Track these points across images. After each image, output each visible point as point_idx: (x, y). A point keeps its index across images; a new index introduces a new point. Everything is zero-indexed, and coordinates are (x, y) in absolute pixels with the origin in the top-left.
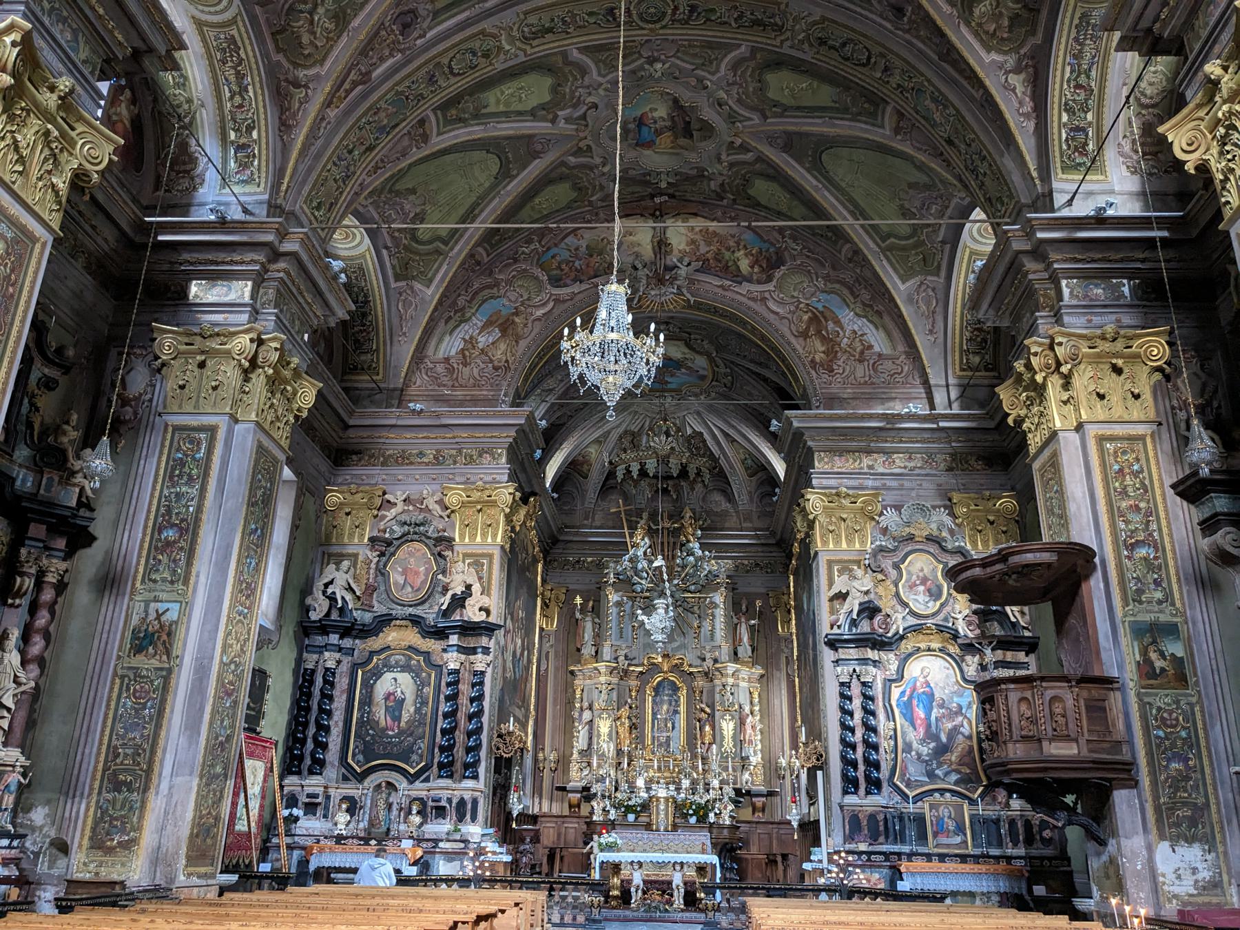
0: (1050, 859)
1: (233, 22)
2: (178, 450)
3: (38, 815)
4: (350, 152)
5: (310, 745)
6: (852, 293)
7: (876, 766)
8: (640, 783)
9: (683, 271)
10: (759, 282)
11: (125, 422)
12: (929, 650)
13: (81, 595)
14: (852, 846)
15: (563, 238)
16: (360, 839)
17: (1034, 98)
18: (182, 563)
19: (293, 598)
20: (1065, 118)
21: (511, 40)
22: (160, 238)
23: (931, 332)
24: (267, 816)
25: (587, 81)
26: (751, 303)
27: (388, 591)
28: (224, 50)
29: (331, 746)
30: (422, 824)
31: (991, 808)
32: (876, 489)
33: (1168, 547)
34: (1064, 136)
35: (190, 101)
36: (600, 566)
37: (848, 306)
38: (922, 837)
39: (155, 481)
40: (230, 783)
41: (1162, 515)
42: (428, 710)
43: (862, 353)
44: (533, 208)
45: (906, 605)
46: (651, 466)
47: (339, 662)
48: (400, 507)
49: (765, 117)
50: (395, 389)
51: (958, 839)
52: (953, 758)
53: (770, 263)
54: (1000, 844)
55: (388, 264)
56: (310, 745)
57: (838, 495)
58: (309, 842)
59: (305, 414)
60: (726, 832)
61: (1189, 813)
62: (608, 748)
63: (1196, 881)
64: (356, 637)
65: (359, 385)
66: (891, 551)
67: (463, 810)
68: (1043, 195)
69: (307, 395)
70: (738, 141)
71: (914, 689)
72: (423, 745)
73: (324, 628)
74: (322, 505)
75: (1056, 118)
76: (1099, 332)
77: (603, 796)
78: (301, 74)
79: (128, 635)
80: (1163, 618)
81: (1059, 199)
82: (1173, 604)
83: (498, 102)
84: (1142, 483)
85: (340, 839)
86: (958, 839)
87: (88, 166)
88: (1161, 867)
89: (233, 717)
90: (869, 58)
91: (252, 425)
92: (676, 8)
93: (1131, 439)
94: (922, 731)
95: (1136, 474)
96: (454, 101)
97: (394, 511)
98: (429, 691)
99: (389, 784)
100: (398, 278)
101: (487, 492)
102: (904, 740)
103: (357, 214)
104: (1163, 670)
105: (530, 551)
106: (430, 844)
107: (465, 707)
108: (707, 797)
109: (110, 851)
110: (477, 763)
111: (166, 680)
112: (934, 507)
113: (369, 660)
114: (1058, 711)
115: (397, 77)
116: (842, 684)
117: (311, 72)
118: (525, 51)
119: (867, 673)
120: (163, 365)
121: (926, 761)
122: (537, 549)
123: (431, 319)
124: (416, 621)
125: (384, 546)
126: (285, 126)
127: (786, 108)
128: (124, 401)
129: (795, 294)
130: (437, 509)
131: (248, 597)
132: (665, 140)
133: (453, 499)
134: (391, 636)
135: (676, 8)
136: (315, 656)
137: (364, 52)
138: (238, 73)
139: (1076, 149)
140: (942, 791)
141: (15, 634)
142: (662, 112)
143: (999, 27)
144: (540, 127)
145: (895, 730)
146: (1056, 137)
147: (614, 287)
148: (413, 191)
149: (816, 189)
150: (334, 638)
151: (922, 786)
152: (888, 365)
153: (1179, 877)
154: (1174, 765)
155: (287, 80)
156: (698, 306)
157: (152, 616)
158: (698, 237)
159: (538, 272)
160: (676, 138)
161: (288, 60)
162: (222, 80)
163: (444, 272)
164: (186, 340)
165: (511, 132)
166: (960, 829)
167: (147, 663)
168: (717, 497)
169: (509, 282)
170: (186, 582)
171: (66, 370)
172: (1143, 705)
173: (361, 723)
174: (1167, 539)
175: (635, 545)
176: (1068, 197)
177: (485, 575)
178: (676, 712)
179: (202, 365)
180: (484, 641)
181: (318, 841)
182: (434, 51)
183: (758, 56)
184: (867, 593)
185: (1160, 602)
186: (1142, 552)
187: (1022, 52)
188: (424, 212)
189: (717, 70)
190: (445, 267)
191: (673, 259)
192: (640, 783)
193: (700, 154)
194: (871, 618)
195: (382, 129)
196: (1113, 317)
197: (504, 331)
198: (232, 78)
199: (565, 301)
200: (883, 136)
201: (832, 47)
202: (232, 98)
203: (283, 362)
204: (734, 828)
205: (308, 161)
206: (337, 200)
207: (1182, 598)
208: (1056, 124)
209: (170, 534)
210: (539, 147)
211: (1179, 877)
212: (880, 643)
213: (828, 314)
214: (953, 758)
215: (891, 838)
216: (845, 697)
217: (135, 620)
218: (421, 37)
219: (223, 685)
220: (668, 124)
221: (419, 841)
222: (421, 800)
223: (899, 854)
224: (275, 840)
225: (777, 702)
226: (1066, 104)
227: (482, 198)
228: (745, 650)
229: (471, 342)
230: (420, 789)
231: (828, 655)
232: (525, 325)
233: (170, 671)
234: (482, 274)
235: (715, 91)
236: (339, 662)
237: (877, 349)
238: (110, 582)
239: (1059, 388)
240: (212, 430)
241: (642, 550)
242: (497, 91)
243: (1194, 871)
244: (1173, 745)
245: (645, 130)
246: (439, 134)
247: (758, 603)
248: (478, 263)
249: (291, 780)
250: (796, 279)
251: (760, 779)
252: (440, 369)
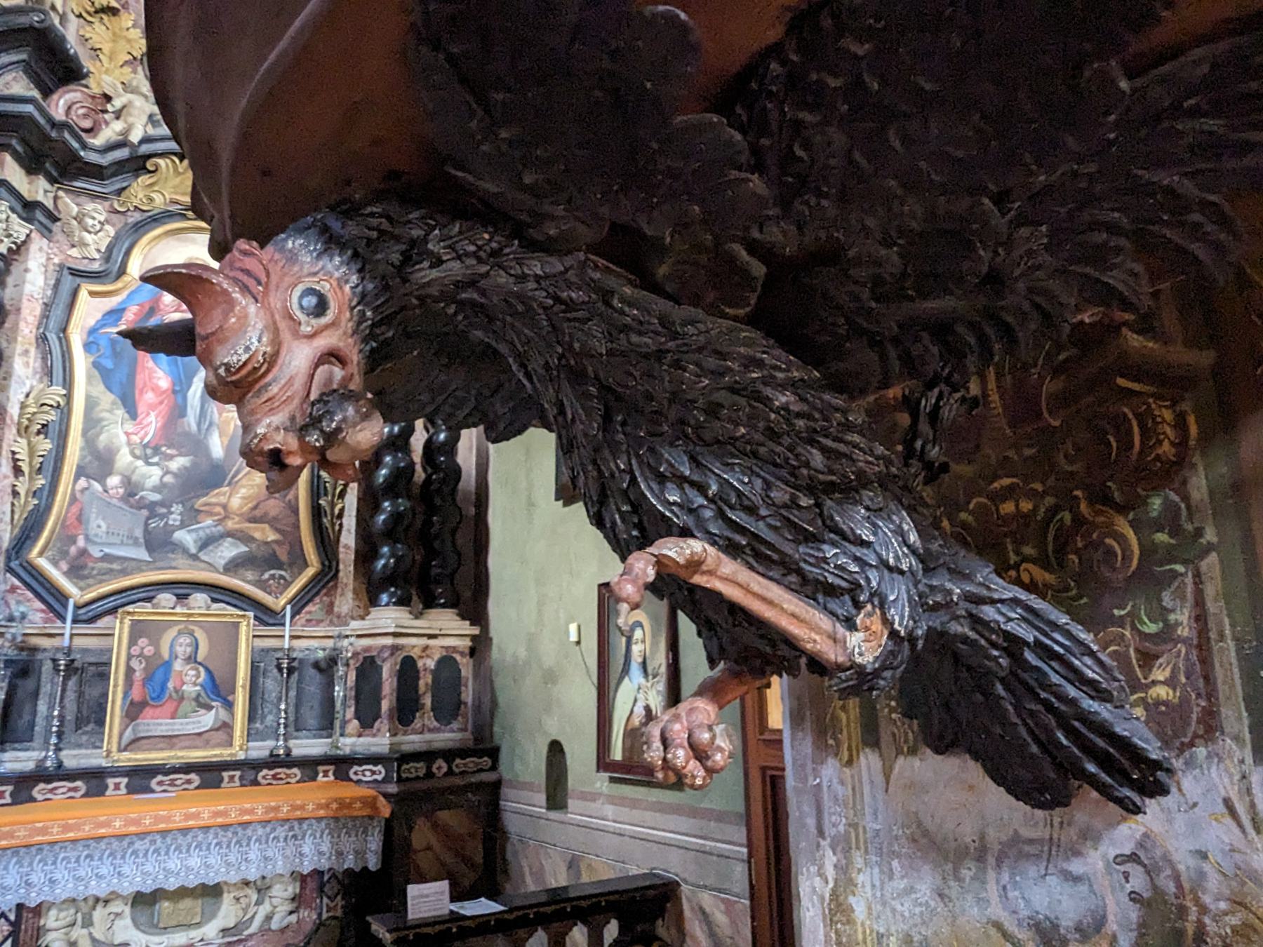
0: (449, 755)
31: (320, 630)
51: (207, 720)
52: (235, 502)
86: (207, 720)
94: (152, 423)
121: (151, 506)
140: (183, 589)
145: (65, 410)
151: (124, 573)
166: (218, 690)
214: (235, 502)
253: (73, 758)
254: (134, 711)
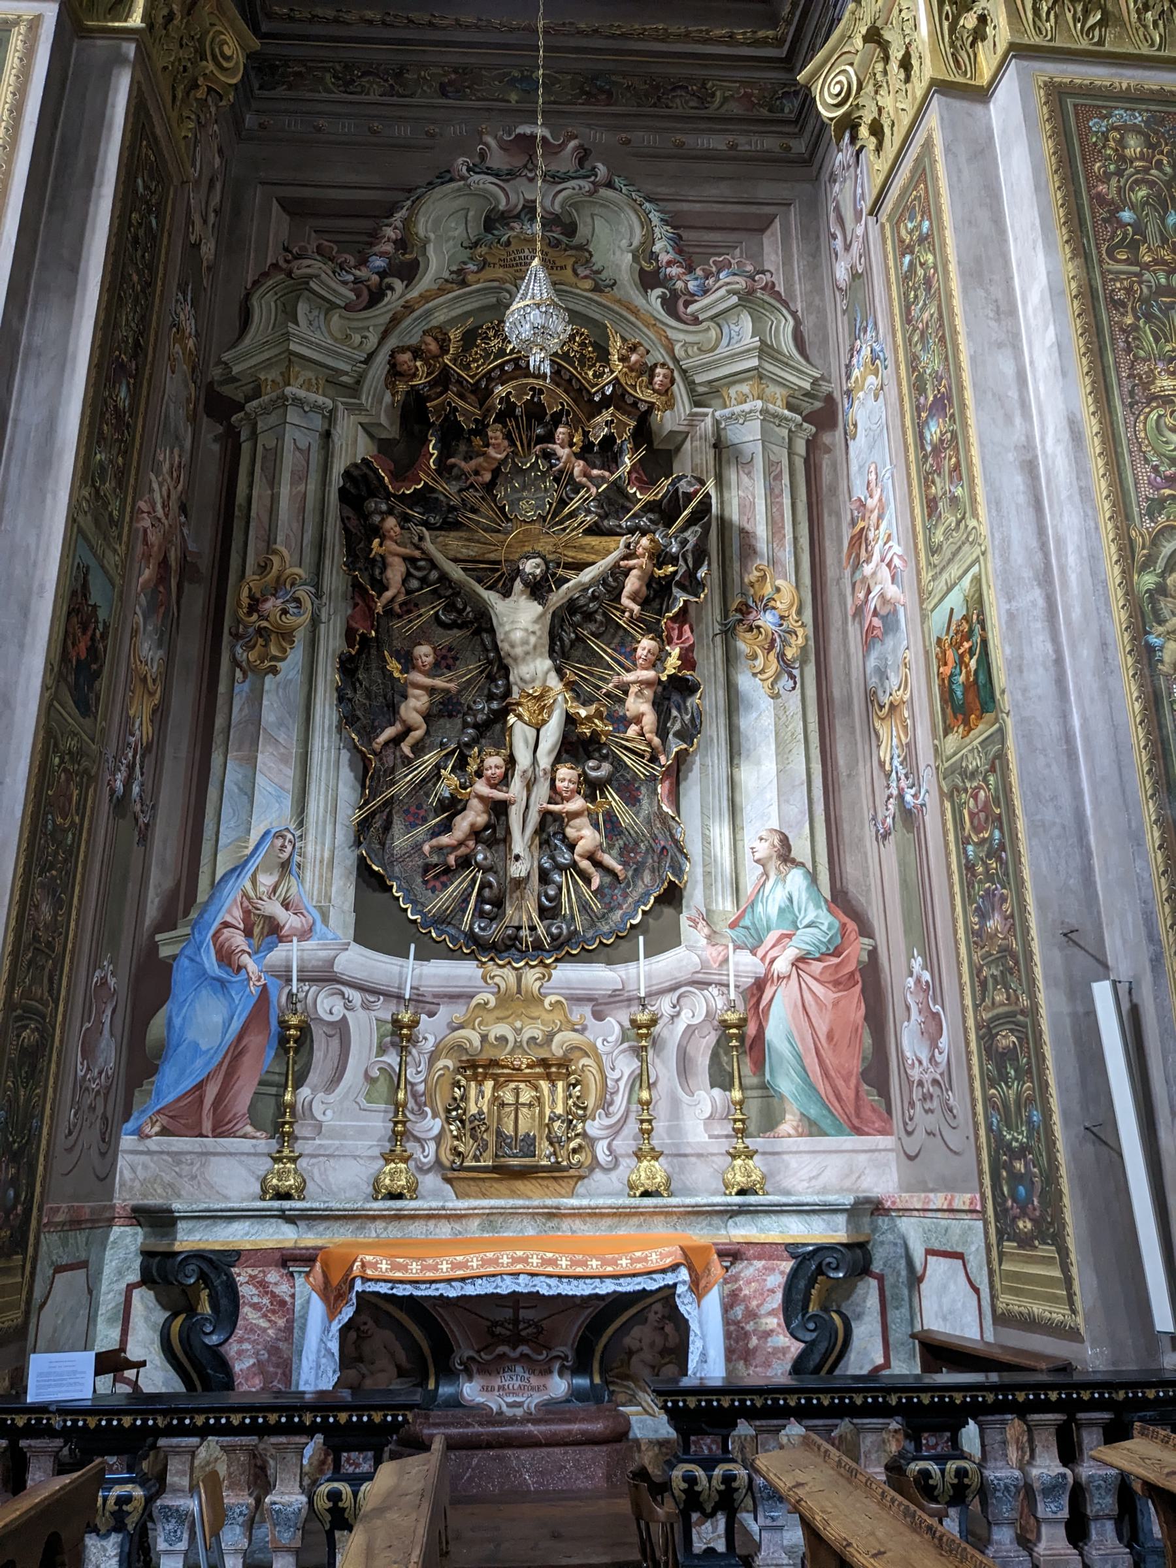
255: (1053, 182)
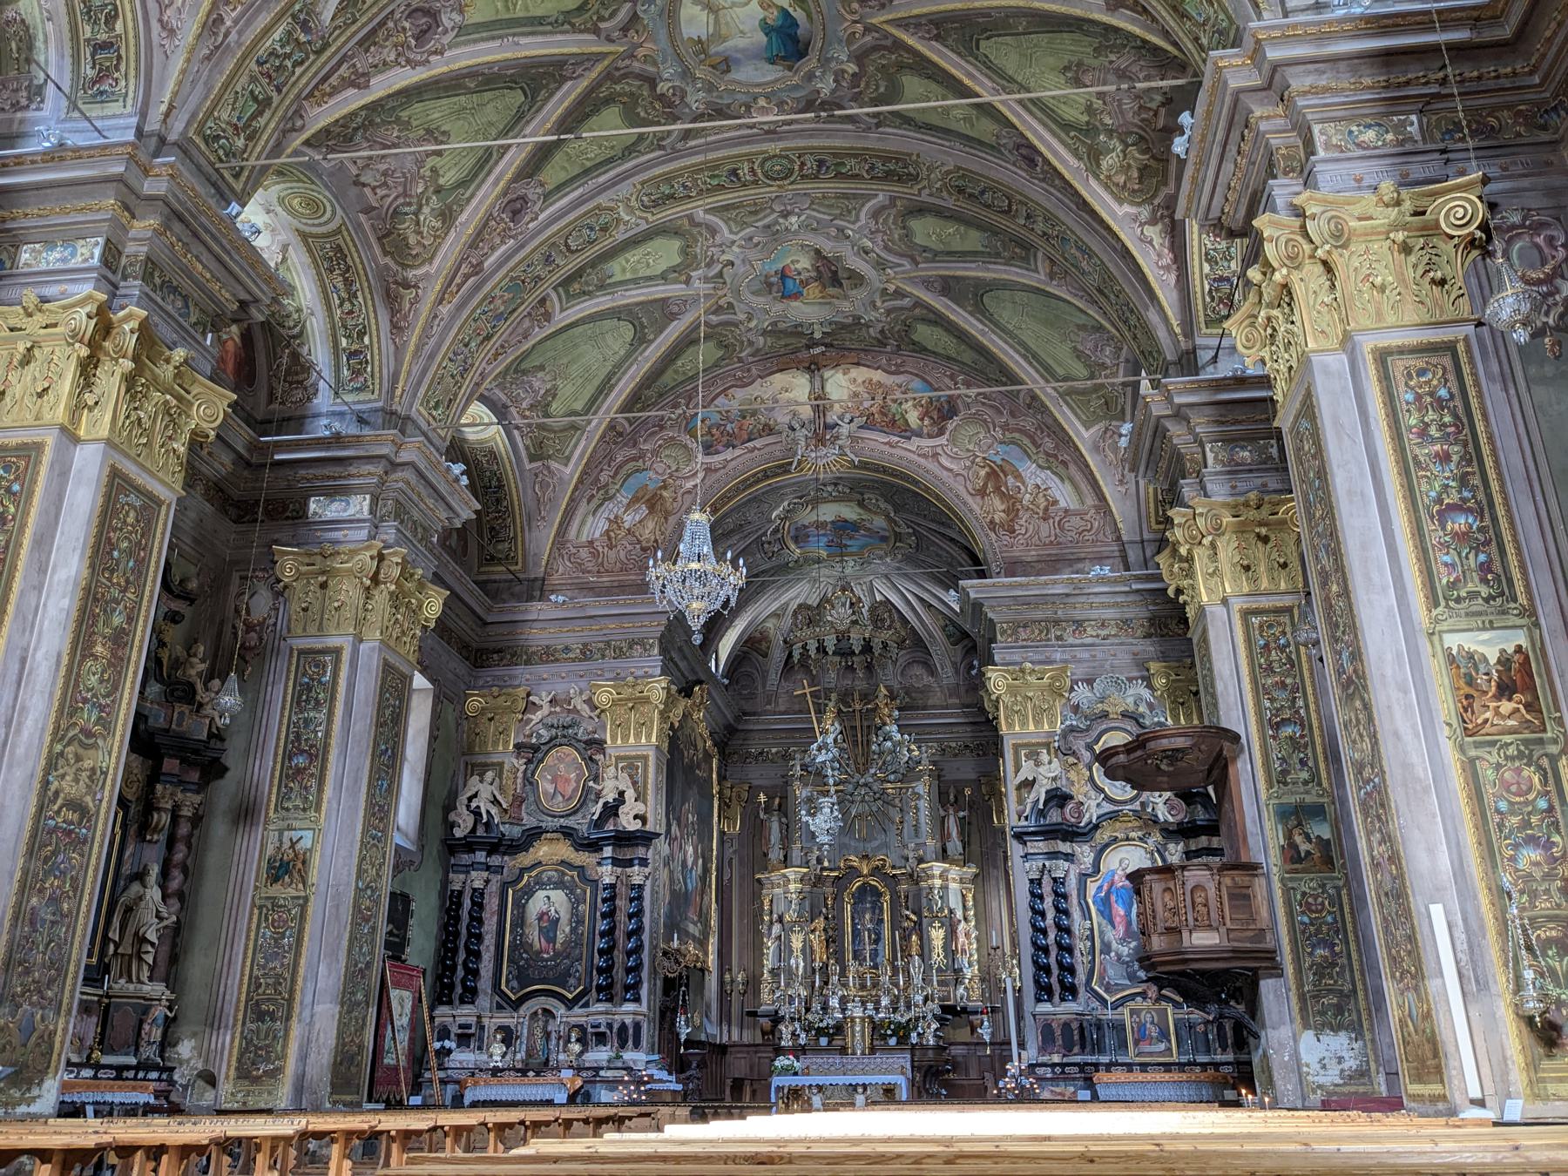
1: (338, 231)
2: (304, 675)
3: (185, 1049)
4: (466, 345)
5: (460, 972)
6: (1034, 443)
7: (1071, 970)
8: (834, 1002)
9: (845, 430)
10: (930, 436)
11: (251, 649)
12: (1127, 839)
13: (219, 828)
14: (1045, 1059)
15: (713, 400)
16: (518, 1071)
17: (1172, 249)
18: (314, 790)
19: (436, 815)
20: (1206, 268)
21: (631, 210)
22: (277, 457)
23: (1121, 482)
24: (418, 1051)
25: (718, 239)
26: (922, 461)
27: (537, 802)
28: (330, 258)
29: (483, 972)
30: (582, 1053)
32: (1066, 661)
33: (1315, 724)
34: (1207, 287)
35: (299, 310)
36: (787, 757)
37: (1029, 457)
38: (1123, 1045)
39: (283, 708)
40: (373, 1011)
41: (1309, 690)
42: (584, 929)
43: (1046, 509)
44: (676, 372)
45: (1102, 791)
46: (830, 643)
47: (487, 881)
48: (546, 709)
49: (917, 264)
50: (536, 579)
51: (1162, 1046)
53: (942, 414)
54: (1208, 1052)
55: (521, 445)
56: (460, 972)
57: (1022, 671)
58: (463, 1076)
59: (432, 625)
60: (931, 1054)
61: (1335, 1001)
62: (798, 963)
63: (1342, 1071)
64: (504, 854)
65: (497, 577)
66: (1082, 731)
67: (625, 1036)
68: (1187, 352)
69: (433, 605)
70: (892, 288)
71: (1112, 884)
72: (581, 967)
73: (469, 845)
74: (463, 711)
75: (1197, 270)
76: (1242, 499)
77: (793, 1019)
78: (411, 274)
79: (264, 865)
80: (1309, 799)
81: (1205, 356)
82: (1320, 784)
83: (624, 270)
84: (1289, 658)
85: (496, 1071)
86: (1162, 1046)
87: (205, 425)
88: (1305, 1058)
89: (372, 942)
90: (1010, 206)
91: (377, 644)
92: (803, 164)
93: (1278, 611)
94: (1121, 929)
95: (1282, 649)
96: (578, 274)
97: (539, 714)
98: (584, 908)
99: (547, 1012)
100: (532, 459)
101: (639, 688)
102: (1102, 941)
103: (483, 399)
104: (1308, 853)
105: (700, 745)
106: (590, 1073)
107: (624, 924)
108: (912, 1014)
109: (256, 1080)
110: (636, 986)
111: (303, 908)
112: (1130, 680)
113: (520, 877)
114: (1199, 900)
115: (511, 263)
116: (1032, 881)
117: (419, 272)
118: (646, 219)
119: (1058, 868)
120: (286, 587)
122: (709, 743)
123: (572, 499)
124: (567, 833)
125: (532, 752)
126: (396, 328)
127: (936, 254)
128: (249, 628)
129: (971, 447)
130: (585, 710)
131: (381, 819)
132: (813, 291)
133: (604, 697)
134: (543, 851)
135: (803, 164)
136: (462, 877)
137: (473, 245)
138: (346, 280)
139: (1221, 300)
141: (155, 870)
142: (804, 263)
143: (1129, 179)
144: (674, 290)
145: (1092, 930)
146: (1198, 289)
147: (696, 516)
148: (542, 368)
149: (984, 334)
150: (481, 856)
152: (1075, 521)
153: (1324, 1067)
154: (1320, 952)
155: (396, 282)
156: (864, 466)
157: (287, 844)
158: (861, 389)
159: (686, 439)
160: (824, 287)
161: (397, 263)
162: (330, 288)
163: (582, 449)
164: (307, 560)
165: (642, 298)
166: (1164, 1035)
167: (285, 891)
168: (918, 670)
169: (655, 453)
170: (318, 809)
171: (192, 602)
172: (1287, 891)
173: (513, 947)
174: (1314, 716)
175: (824, 732)
176: (1212, 353)
177: (640, 779)
178: (882, 921)
179: (324, 586)
180: (641, 852)
181: (473, 1075)
182: (549, 232)
183: (899, 203)
184: (1054, 779)
185: (1306, 783)
186: (1288, 731)
187: (1156, 202)
188: (555, 387)
189: (857, 220)
190: (583, 443)
191: (832, 417)
192: (834, 1002)
193: (851, 304)
194: (1062, 806)
195: (499, 317)
196: (1259, 481)
197: (652, 508)
198: (340, 285)
199: (716, 470)
200: (1039, 281)
201: (971, 195)
202: (341, 305)
203: (406, 575)
204: (939, 1049)
205: (422, 362)
206: (456, 395)
207: (1329, 778)
208: (1197, 276)
209: (301, 761)
210: (676, 309)
211: (1324, 1067)
212: (1070, 833)
213: (1007, 468)
215: (1088, 1049)
216: (1036, 896)
217: (270, 850)
218: (532, 220)
219: (360, 911)
220: (814, 274)
221: (579, 1069)
222: (581, 1028)
223: (1096, 1066)
224: (427, 1075)
225: (995, 904)
226: (1207, 254)
227: (618, 366)
228: (955, 846)
229: (616, 521)
230: (578, 1015)
231: (1015, 849)
232: (675, 500)
233: (306, 899)
234: (625, 445)
235: (858, 240)
236: (487, 881)
237: (1063, 504)
238: (246, 813)
239: (1206, 560)
240: (337, 652)
241: (832, 736)
242: (621, 260)
243: (1340, 1060)
244: (1318, 931)
245: (790, 283)
246: (562, 310)
247: (968, 792)
248: (620, 434)
249: (442, 1010)
250: (971, 430)
251: (976, 994)
252: (584, 553)
253: (1121, 1059)
254: (1137, 1042)
255: (96, 521)
